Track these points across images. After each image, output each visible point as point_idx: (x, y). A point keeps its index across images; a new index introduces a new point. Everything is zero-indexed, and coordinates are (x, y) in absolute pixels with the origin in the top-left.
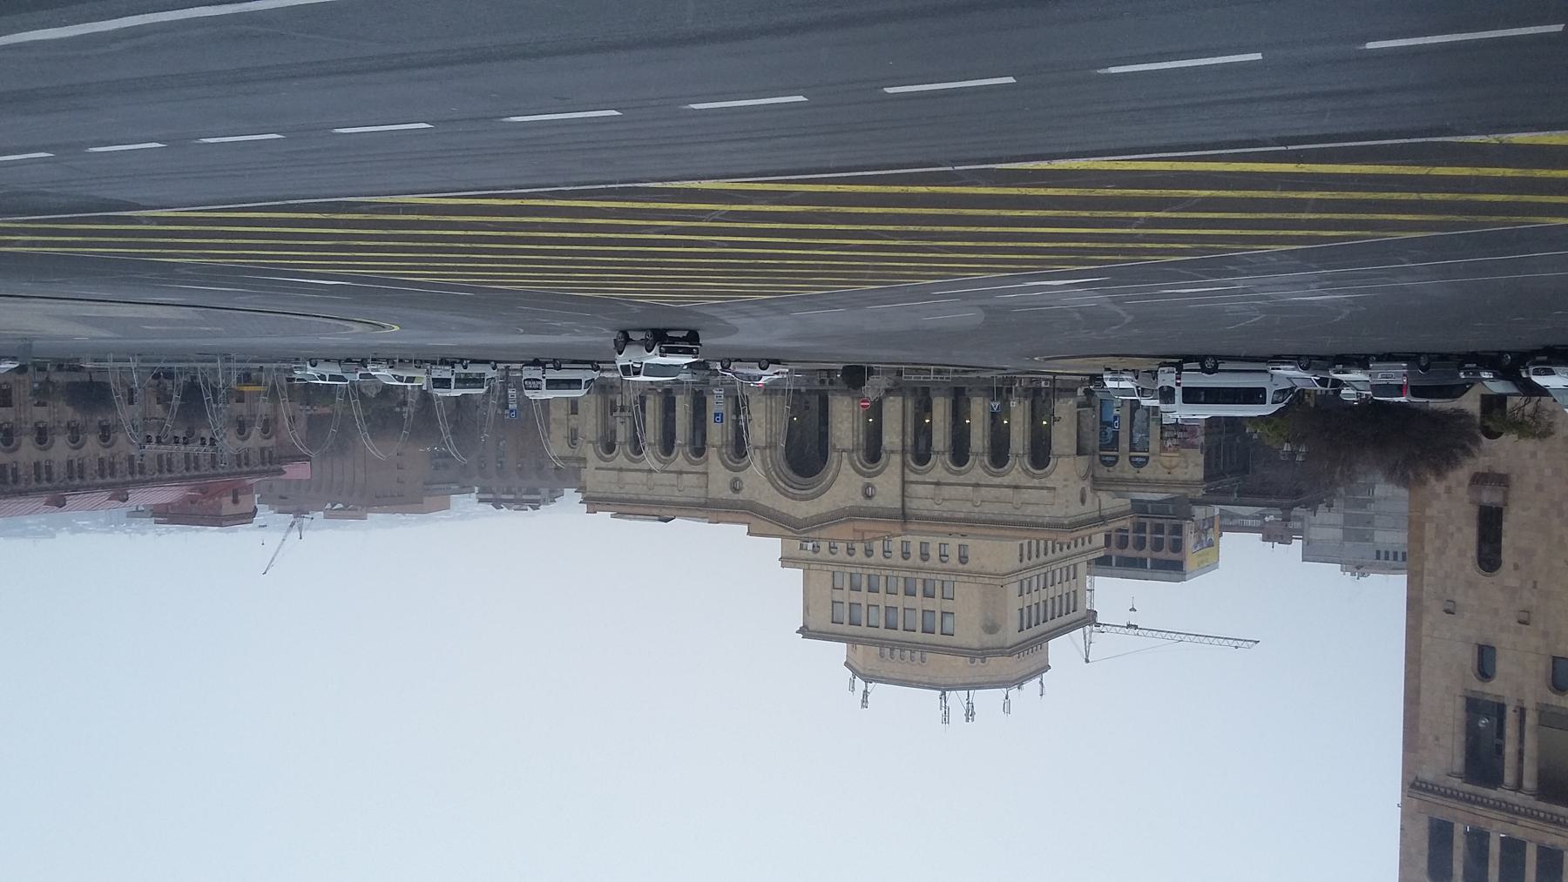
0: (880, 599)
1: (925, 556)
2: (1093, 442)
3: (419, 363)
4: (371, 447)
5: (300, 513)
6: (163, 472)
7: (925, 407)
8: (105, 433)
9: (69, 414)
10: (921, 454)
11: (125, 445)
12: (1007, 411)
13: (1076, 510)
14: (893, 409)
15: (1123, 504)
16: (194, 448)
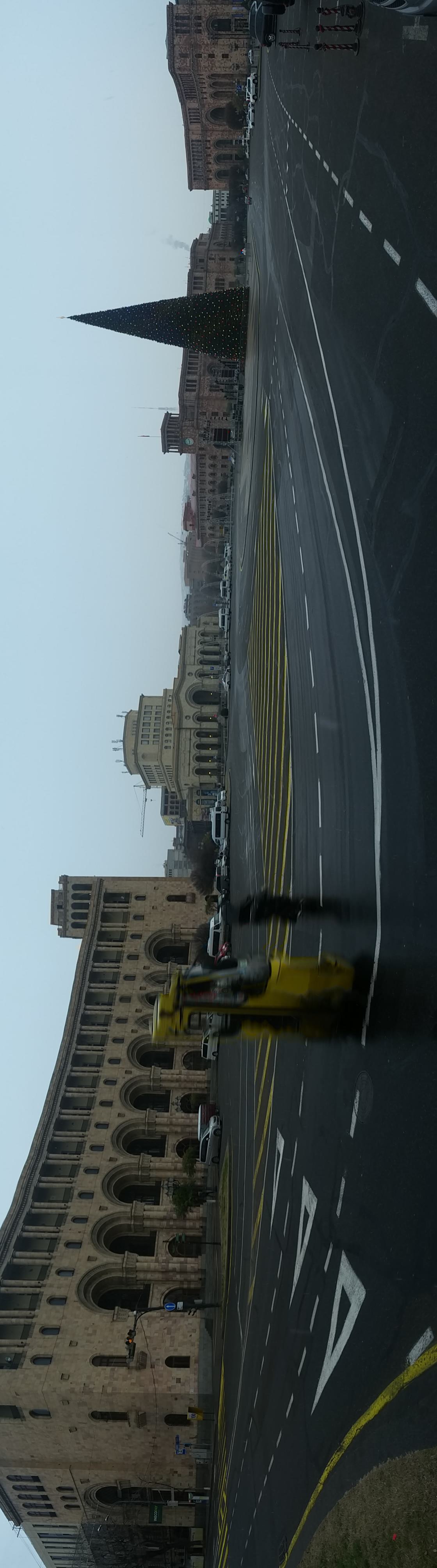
0: (153, 721)
1: (167, 735)
2: (204, 788)
3: (231, 578)
4: (205, 564)
5: (186, 544)
6: (200, 506)
7: (215, 735)
8: (213, 491)
9: (219, 482)
10: (199, 734)
11: (209, 496)
12: (213, 761)
13: (182, 783)
14: (214, 726)
15: (185, 798)
16: (207, 514)
